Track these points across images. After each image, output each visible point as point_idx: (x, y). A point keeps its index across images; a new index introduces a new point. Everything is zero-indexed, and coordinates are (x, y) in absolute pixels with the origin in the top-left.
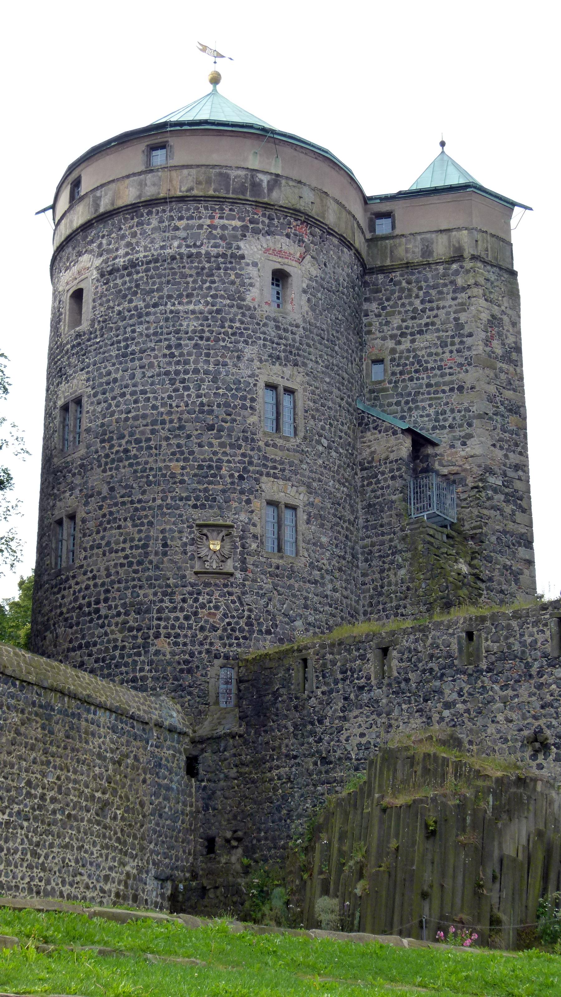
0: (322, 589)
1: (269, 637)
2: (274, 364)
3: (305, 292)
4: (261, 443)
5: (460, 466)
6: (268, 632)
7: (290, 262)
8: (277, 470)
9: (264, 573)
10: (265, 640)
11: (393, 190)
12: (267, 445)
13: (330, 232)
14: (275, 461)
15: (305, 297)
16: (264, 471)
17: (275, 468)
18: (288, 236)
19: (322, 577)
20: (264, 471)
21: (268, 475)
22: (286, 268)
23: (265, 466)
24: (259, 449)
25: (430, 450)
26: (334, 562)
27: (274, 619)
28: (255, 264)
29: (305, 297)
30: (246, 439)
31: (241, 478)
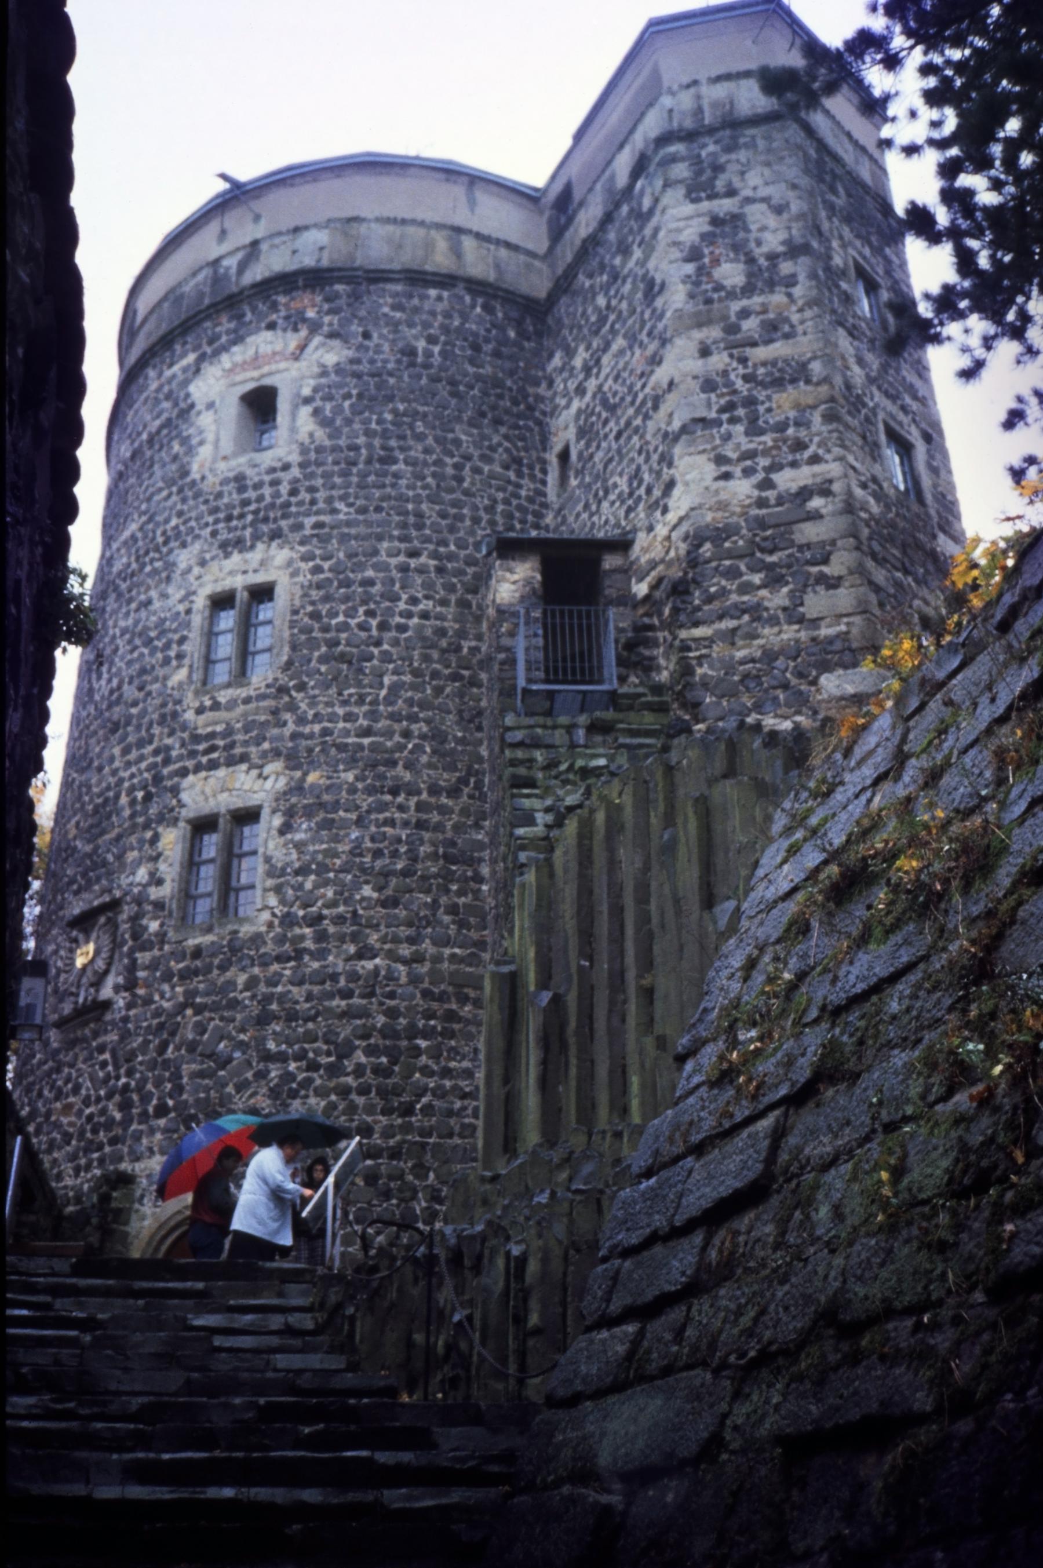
0: (316, 965)
1: (162, 1122)
2: (227, 555)
3: (307, 401)
4: (189, 716)
5: (662, 561)
6: (162, 1110)
7: (274, 367)
8: (221, 752)
9: (168, 977)
10: (152, 1131)
11: (567, 142)
12: (200, 711)
13: (377, 277)
14: (212, 735)
15: (305, 411)
16: (190, 764)
17: (213, 749)
18: (272, 326)
19: (321, 937)
20: (190, 764)
21: (198, 769)
22: (267, 381)
23: (193, 754)
24: (184, 728)
25: (610, 562)
26: (367, 891)
27: (176, 1076)
28: (211, 406)
29: (305, 411)
30: (162, 720)
31: (148, 798)
